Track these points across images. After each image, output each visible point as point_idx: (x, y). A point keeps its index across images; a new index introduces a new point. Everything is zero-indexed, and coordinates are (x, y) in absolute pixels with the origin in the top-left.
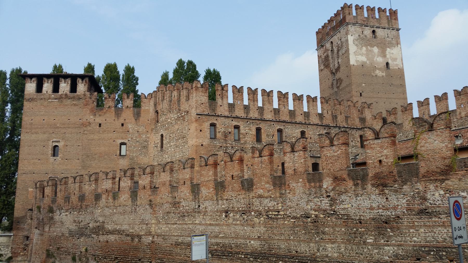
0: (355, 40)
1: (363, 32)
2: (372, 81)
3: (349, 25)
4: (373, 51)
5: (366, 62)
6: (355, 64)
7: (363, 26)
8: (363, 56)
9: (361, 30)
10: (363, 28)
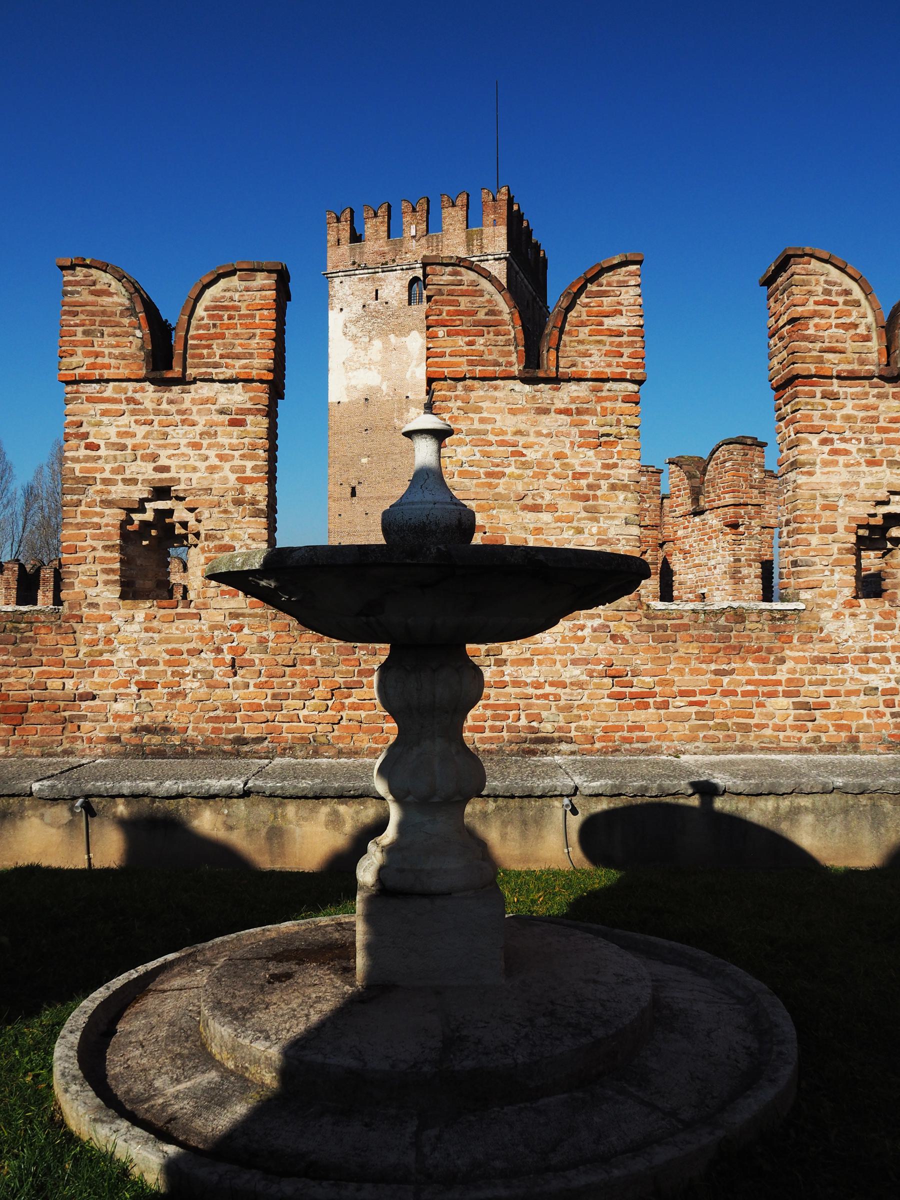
0: (348, 325)
1: (377, 291)
2: (394, 444)
3: (335, 279)
4: (406, 348)
5: (379, 389)
6: (344, 399)
7: (378, 272)
8: (370, 369)
9: (370, 288)
10: (380, 279)
